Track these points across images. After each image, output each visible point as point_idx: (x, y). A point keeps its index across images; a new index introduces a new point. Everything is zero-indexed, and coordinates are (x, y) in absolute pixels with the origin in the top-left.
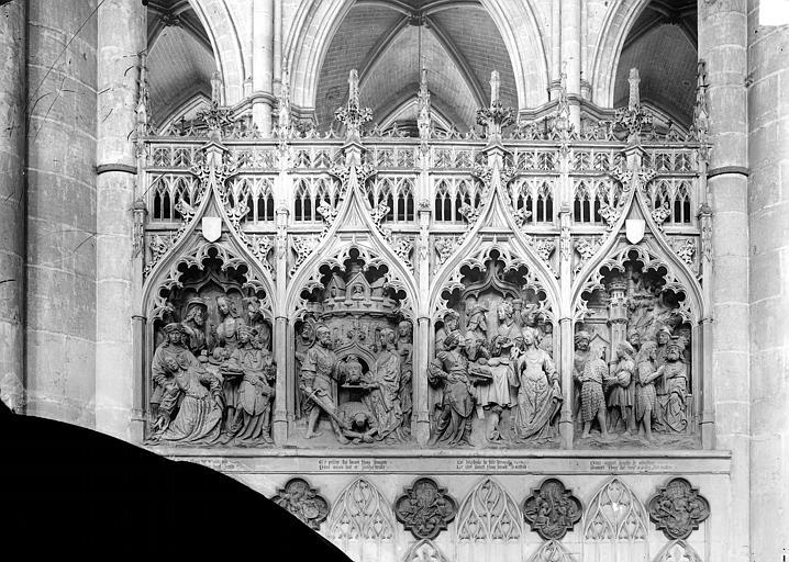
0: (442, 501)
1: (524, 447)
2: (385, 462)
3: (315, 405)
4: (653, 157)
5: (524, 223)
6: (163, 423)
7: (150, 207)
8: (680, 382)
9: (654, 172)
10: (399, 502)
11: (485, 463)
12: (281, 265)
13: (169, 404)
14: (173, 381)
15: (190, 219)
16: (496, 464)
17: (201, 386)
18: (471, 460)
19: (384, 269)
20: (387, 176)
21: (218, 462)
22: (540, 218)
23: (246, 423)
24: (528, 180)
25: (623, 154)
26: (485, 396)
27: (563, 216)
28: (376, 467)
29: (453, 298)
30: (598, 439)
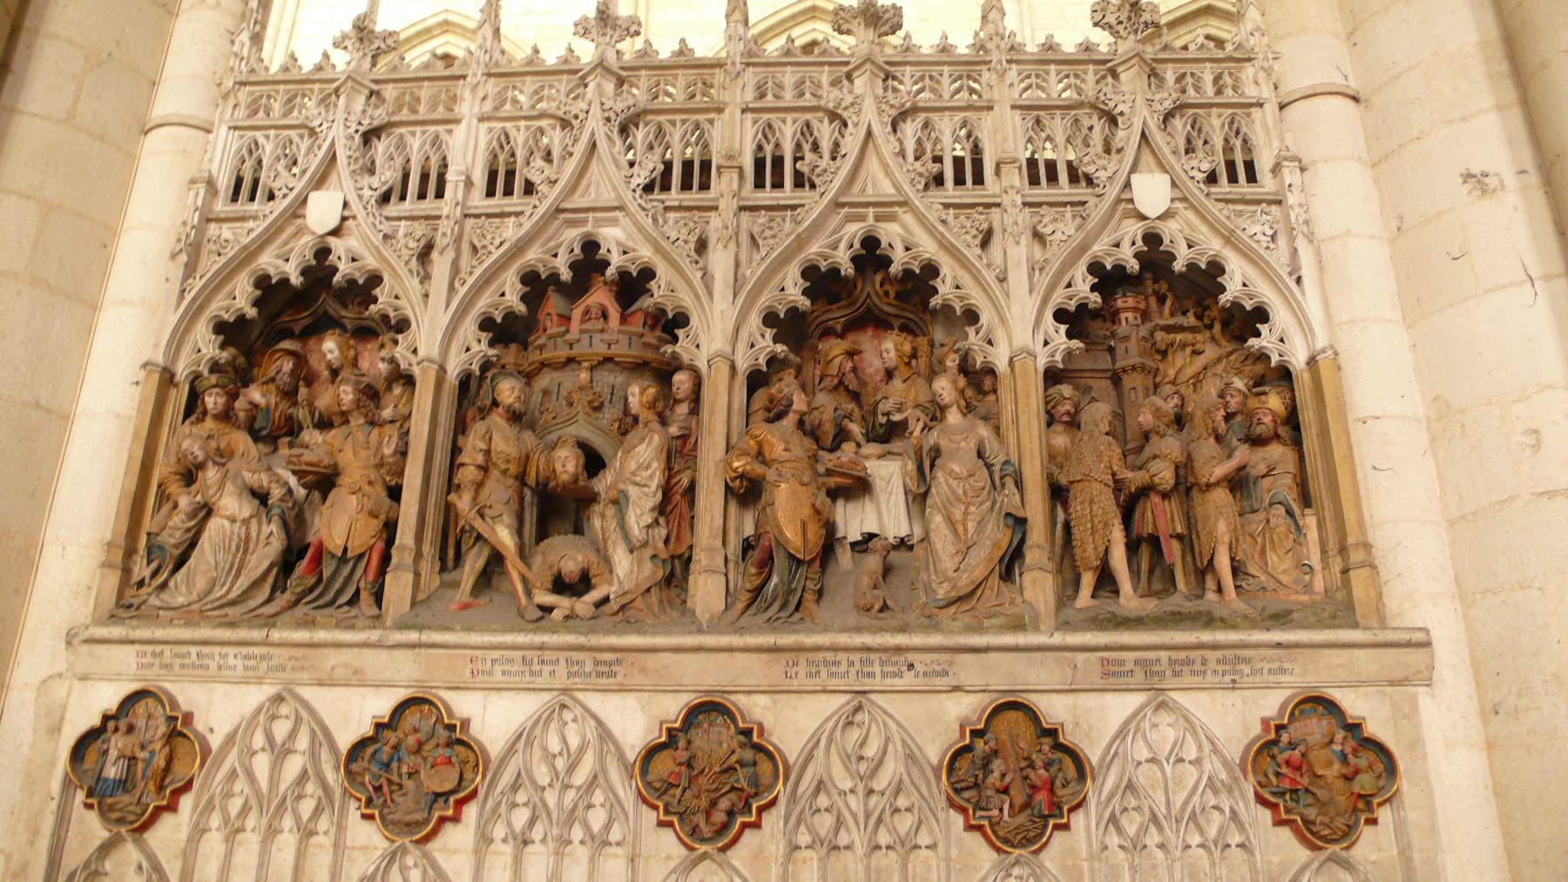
0: (748, 755)
1: (933, 626)
2: (619, 662)
3: (479, 537)
4: (1170, 76)
5: (926, 187)
6: (155, 574)
7: (224, 182)
8: (1283, 487)
9: (1175, 95)
10: (651, 753)
11: (852, 664)
12: (441, 265)
15: (285, 196)
16: (877, 669)
17: (247, 497)
18: (819, 656)
19: (648, 274)
20: (662, 118)
22: (959, 181)
23: (326, 574)
24: (934, 116)
25: (1114, 74)
26: (853, 521)
27: (1005, 169)
28: (600, 675)
29: (788, 325)
30: (1113, 608)
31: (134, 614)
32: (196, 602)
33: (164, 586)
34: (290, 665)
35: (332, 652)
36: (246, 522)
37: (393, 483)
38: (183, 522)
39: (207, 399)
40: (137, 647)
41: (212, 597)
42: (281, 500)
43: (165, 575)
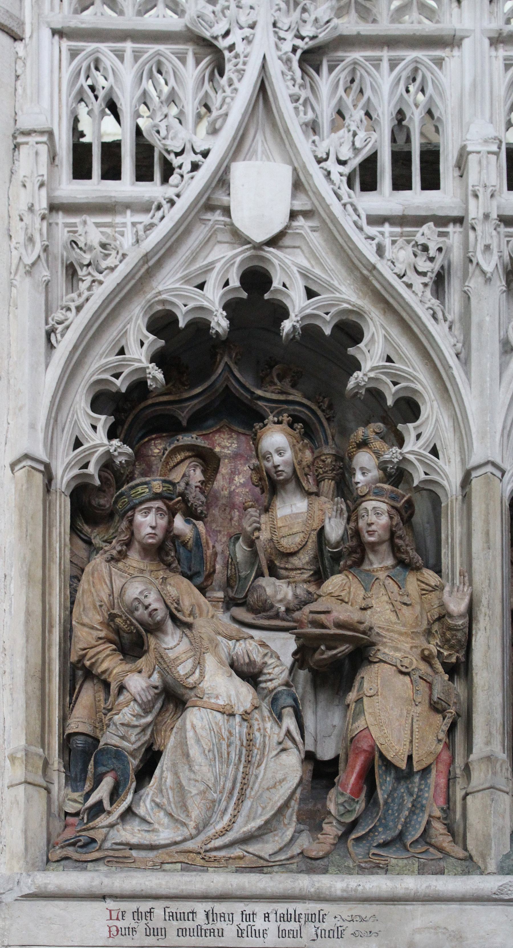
13: (133, 735)
14: (142, 662)
21: (297, 918)
23: (381, 795)
31: (97, 855)
32: (192, 838)
33: (129, 812)
34: (351, 927)
35: (418, 909)
36: (246, 717)
37: (453, 660)
38: (138, 716)
39: (139, 518)
40: (111, 904)
41: (211, 831)
42: (287, 684)
43: (130, 797)
